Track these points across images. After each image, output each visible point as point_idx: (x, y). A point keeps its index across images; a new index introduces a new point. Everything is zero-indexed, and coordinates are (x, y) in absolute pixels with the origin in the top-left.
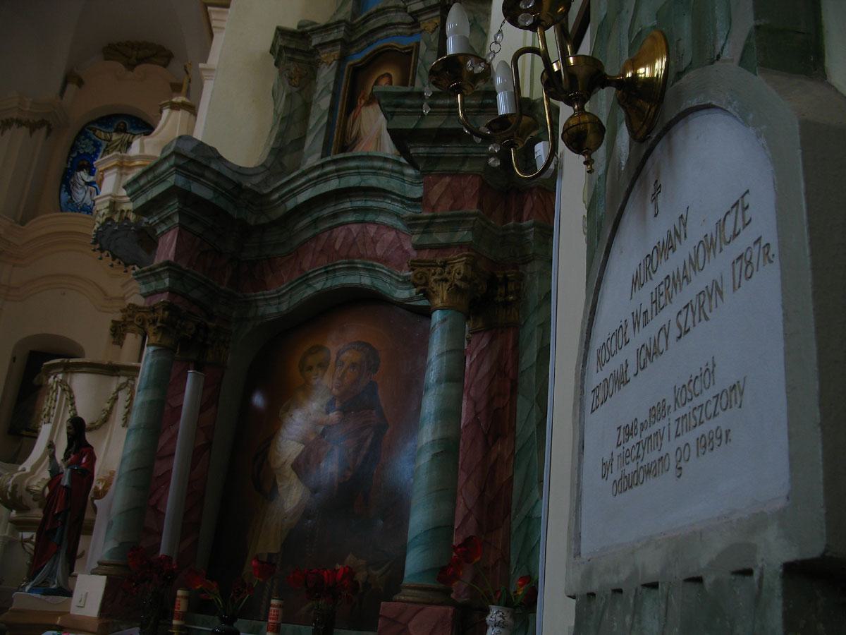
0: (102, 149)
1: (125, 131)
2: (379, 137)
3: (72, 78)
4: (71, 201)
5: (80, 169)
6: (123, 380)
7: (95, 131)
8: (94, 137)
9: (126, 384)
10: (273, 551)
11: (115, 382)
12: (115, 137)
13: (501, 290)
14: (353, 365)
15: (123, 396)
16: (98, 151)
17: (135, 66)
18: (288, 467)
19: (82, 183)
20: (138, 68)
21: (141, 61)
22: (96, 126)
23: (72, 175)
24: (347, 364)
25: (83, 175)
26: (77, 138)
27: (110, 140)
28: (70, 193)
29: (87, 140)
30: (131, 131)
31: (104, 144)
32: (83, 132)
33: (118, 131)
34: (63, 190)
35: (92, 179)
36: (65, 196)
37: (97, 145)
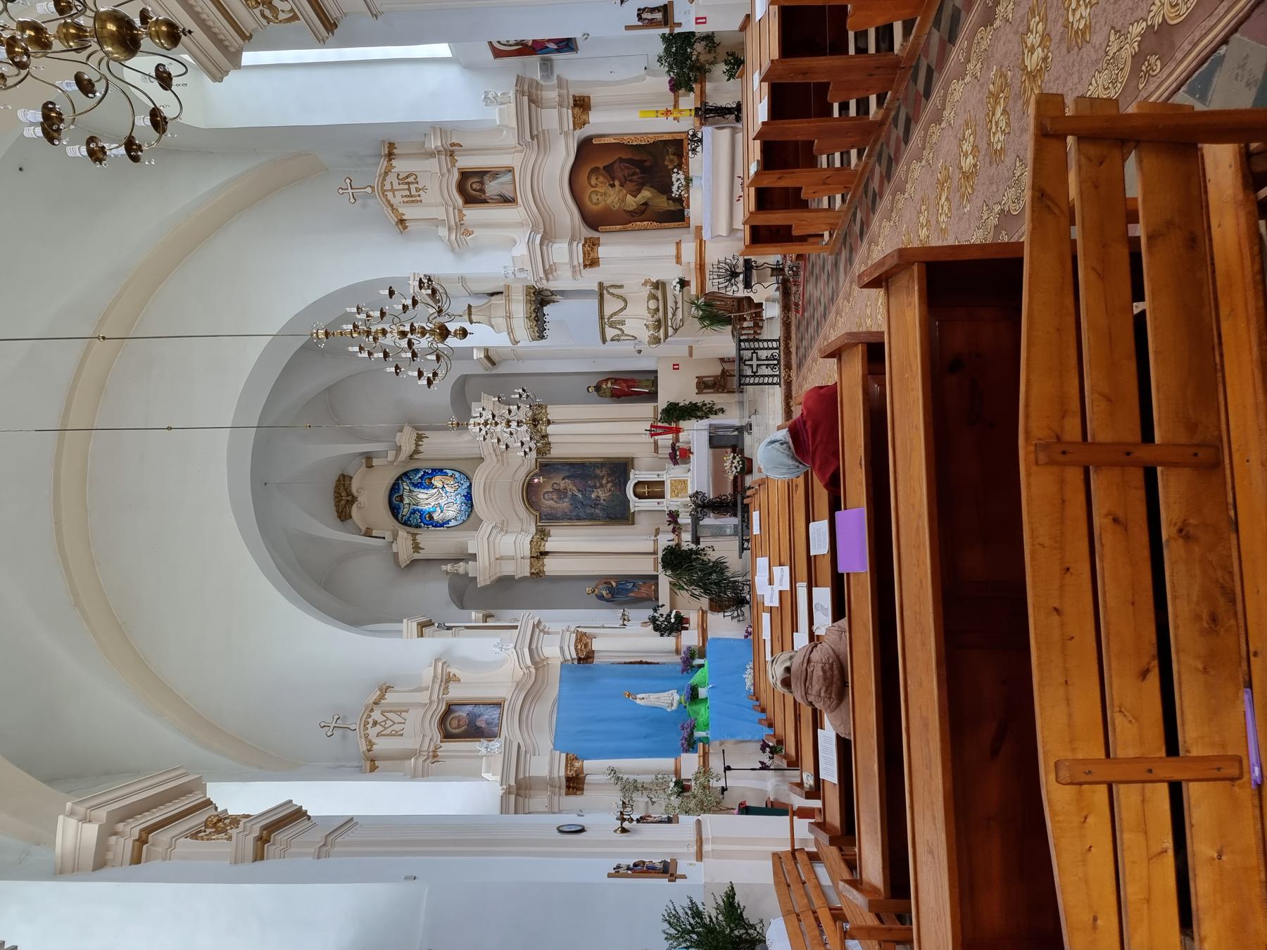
0: (416, 507)
1: (401, 497)
2: (502, 184)
3: (368, 533)
4: (455, 519)
5: (431, 518)
6: (605, 291)
7: (404, 516)
8: (408, 515)
9: (606, 290)
10: (665, 197)
11: (606, 296)
12: (406, 501)
13: (579, 102)
14: (597, 179)
15: (611, 290)
16: (418, 510)
17: (353, 497)
18: (635, 199)
19: (442, 514)
20: (355, 493)
21: (349, 494)
22: (400, 516)
23: (437, 522)
24: (597, 182)
25: (436, 516)
26: (410, 526)
27: (409, 504)
28: (449, 520)
29: (411, 519)
30: (401, 492)
31: (412, 507)
32: (405, 524)
33: (401, 500)
34: (447, 525)
35: (438, 509)
36: (451, 524)
37: (414, 512)
